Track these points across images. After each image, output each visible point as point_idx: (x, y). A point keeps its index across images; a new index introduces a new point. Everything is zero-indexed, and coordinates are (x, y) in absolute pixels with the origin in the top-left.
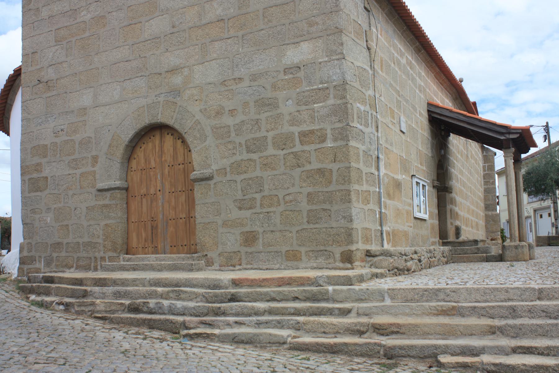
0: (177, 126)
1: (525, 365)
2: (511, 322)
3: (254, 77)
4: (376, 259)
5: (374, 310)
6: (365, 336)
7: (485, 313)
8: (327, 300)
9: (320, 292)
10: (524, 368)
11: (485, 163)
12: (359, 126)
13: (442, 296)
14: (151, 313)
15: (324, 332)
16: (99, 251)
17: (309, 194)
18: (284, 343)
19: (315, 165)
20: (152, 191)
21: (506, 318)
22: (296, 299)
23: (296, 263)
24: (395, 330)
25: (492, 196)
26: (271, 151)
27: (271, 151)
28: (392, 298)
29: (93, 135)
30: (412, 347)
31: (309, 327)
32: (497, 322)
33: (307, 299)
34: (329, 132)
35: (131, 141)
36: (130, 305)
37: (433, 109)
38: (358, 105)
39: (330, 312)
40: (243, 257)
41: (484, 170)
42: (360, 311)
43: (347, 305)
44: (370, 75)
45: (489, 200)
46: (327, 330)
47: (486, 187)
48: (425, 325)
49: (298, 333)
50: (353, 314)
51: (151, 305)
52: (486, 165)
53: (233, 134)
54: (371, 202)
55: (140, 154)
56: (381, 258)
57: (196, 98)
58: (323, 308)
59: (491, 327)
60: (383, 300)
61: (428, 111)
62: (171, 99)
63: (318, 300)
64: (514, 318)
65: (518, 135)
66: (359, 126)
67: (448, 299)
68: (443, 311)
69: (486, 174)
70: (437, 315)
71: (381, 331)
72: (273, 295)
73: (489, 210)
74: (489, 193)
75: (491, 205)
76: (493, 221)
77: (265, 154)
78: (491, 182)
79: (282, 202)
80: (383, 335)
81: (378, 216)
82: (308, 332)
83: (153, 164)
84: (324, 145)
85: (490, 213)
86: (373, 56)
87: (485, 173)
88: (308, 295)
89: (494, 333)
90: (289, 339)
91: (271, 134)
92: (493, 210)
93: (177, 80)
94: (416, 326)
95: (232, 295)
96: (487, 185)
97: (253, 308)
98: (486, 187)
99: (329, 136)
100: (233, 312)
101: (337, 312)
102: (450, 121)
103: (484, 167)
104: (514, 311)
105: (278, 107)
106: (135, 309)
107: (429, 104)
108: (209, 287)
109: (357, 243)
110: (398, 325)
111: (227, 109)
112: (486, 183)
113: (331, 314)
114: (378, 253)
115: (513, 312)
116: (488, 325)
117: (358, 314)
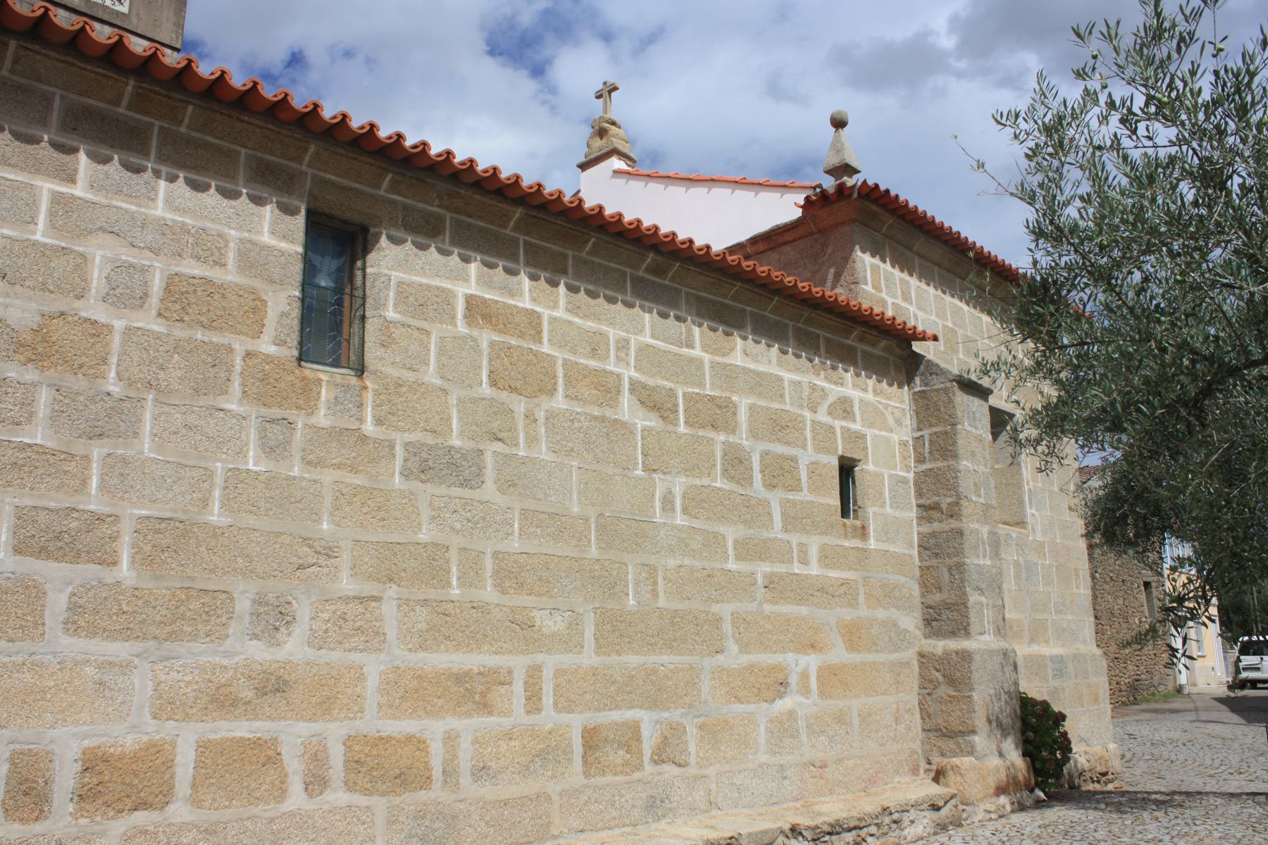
11: (920, 429)
25: (950, 569)
41: (920, 460)
45: (940, 589)
47: (926, 528)
52: (926, 433)
69: (926, 473)
74: (937, 555)
75: (949, 606)
76: (951, 682)
78: (944, 506)
85: (940, 646)
87: (924, 467)
92: (953, 634)
96: (930, 520)
112: (928, 510)
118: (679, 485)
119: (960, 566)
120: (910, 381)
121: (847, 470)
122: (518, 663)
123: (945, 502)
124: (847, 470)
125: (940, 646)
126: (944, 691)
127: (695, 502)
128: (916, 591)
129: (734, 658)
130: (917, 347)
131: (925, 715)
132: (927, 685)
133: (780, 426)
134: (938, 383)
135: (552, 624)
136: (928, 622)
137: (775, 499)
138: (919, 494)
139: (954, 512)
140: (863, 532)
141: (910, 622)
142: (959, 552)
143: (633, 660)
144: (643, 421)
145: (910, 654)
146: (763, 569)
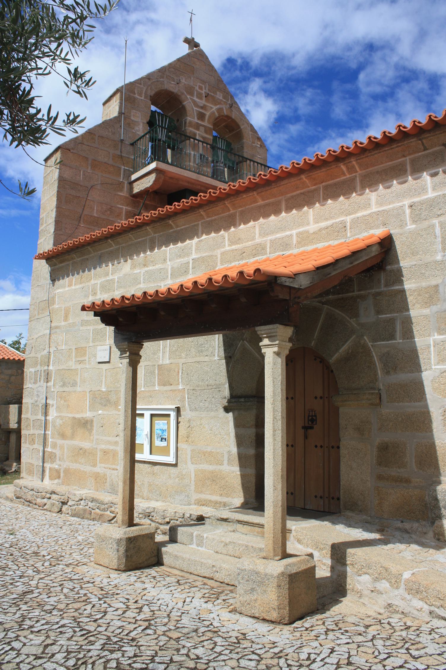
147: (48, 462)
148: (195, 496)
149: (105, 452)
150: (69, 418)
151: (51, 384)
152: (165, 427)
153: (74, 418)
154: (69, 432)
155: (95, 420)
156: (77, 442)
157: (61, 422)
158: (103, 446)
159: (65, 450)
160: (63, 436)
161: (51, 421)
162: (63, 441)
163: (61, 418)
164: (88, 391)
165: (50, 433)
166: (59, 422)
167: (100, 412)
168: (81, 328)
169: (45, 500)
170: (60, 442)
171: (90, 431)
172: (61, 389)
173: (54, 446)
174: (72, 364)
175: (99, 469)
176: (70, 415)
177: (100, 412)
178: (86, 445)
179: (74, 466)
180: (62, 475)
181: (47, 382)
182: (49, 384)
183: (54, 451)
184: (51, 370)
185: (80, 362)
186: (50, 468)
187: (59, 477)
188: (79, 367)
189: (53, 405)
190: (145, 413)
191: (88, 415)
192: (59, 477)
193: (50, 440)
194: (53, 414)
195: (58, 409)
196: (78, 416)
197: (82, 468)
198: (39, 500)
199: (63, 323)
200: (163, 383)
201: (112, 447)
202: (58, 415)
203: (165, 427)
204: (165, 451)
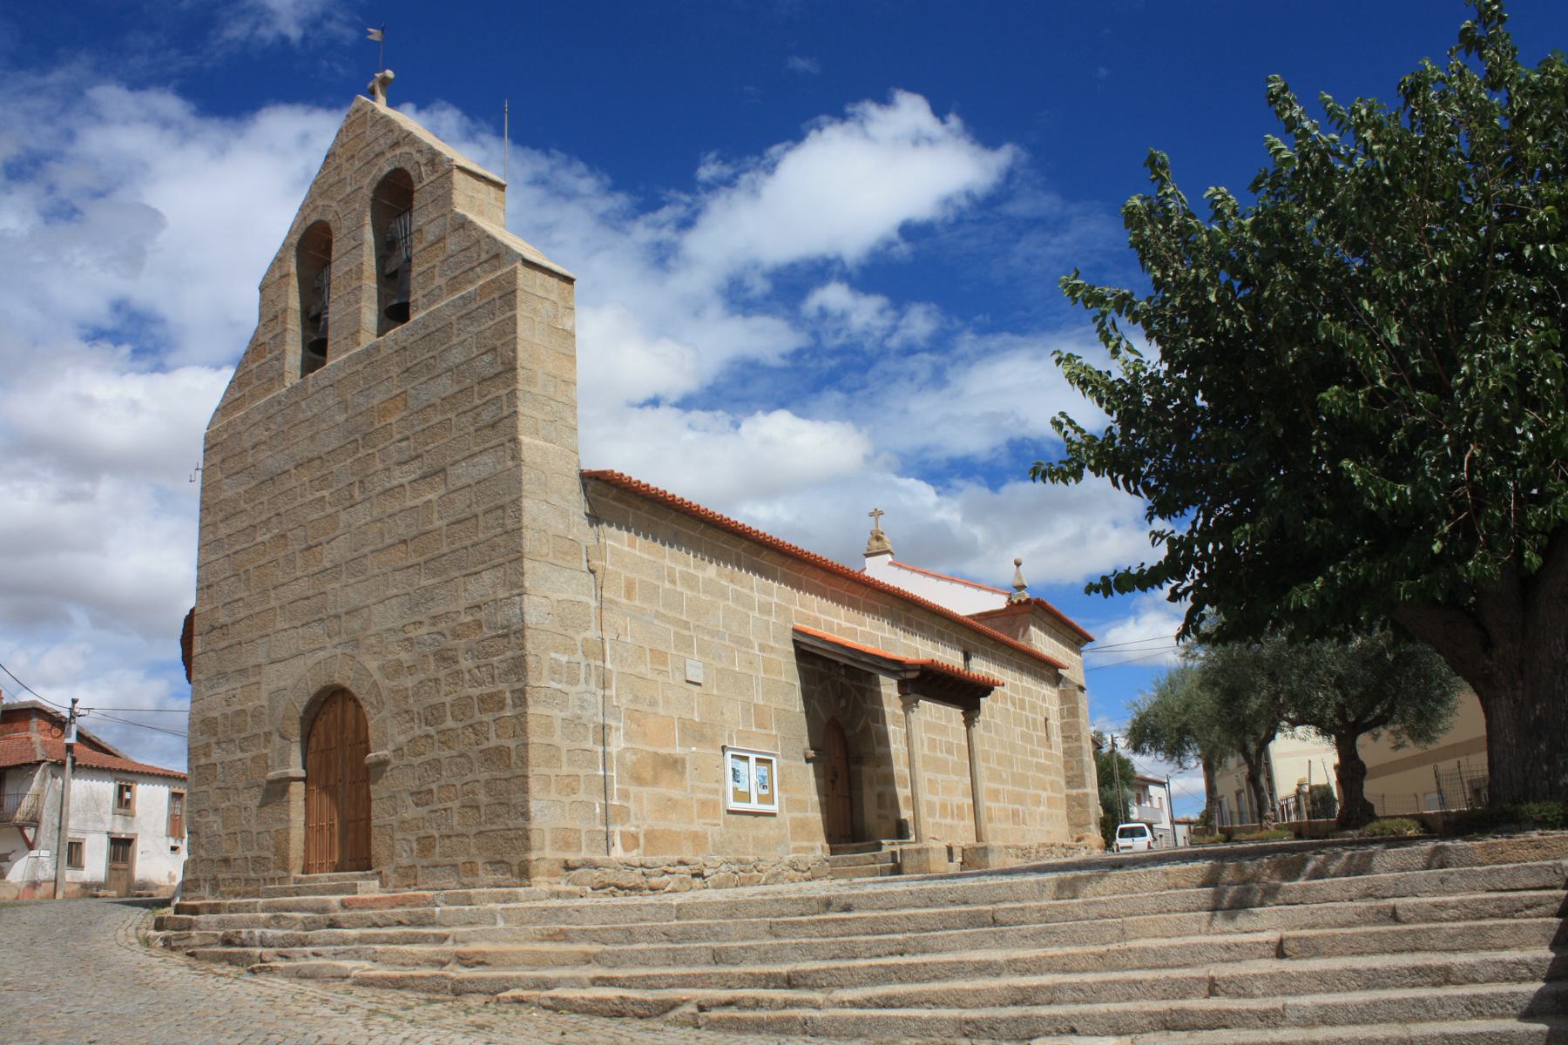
0: (353, 690)
1: (583, 998)
2: (625, 947)
3: (435, 619)
4: (574, 873)
5: (473, 936)
6: (447, 967)
7: (597, 938)
8: (433, 924)
9: (427, 915)
10: (581, 1002)
12: (554, 685)
13: (563, 917)
14: (243, 945)
15: (403, 964)
16: (268, 870)
17: (487, 782)
18: (347, 977)
19: (494, 742)
20: (332, 782)
21: (622, 943)
22: (400, 923)
23: (471, 879)
24: (481, 959)
26: (450, 723)
27: (450, 723)
28: (506, 920)
29: (266, 703)
30: (482, 980)
31: (386, 957)
32: (596, 948)
33: (411, 924)
34: (508, 695)
35: (307, 710)
36: (224, 936)
37: (800, 638)
38: (553, 655)
39: (424, 939)
40: (420, 873)
41: (1062, 718)
42: (457, 938)
43: (445, 931)
44: (592, 610)
46: (406, 961)
47: (1066, 746)
48: (513, 953)
49: (376, 965)
50: (450, 942)
51: (244, 936)
53: (411, 700)
54: (582, 790)
55: (320, 727)
56: (582, 870)
57: (375, 649)
58: (418, 934)
59: (587, 954)
60: (495, 924)
61: (795, 641)
62: (348, 651)
63: (423, 925)
64: (630, 943)
65: (917, 674)
66: (554, 685)
67: (570, 920)
68: (549, 935)
70: (542, 941)
71: (465, 962)
72: (376, 919)
73: (1073, 787)
76: (1080, 805)
77: (443, 727)
79: (460, 794)
80: (467, 966)
81: (598, 810)
82: (386, 963)
83: (333, 744)
84: (503, 713)
85: (1074, 792)
86: (599, 580)
88: (413, 918)
89: (589, 962)
90: (355, 972)
91: (448, 700)
92: (1079, 787)
93: (356, 624)
94: (504, 954)
95: (331, 920)
97: (342, 936)
98: (1066, 746)
99: (509, 701)
100: (321, 940)
101: (432, 939)
102: (826, 655)
103: (1062, 710)
104: (631, 933)
105: (457, 662)
106: (228, 942)
107: (795, 631)
108: (317, 911)
109: (541, 849)
110: (484, 954)
111: (405, 665)
113: (426, 942)
114: (577, 864)
115: (630, 935)
116: (582, 952)
117: (455, 942)
118: (1018, 730)
119: (1081, 761)
120: (1057, 685)
121: (1046, 720)
122: (1001, 787)
123: (1074, 735)
124: (1046, 720)
125: (1074, 792)
126: (1077, 809)
127: (1025, 737)
128: (1062, 770)
129: (1032, 791)
130: (1060, 671)
131: (1069, 819)
132: (1070, 807)
133: (1033, 707)
134: (1070, 687)
135: (1005, 776)
136: (1068, 783)
137: (1034, 734)
138: (1063, 731)
139: (1078, 739)
140: (1051, 748)
141: (1063, 783)
142: (1081, 755)
143: (1017, 789)
144: (1012, 709)
145: (1063, 796)
146: (1035, 760)
147: (615, 823)
148: (792, 845)
149: (703, 803)
150: (648, 752)
151: (612, 692)
152: (766, 774)
153: (656, 754)
154: (648, 774)
155: (687, 758)
156: (662, 790)
157: (634, 757)
158: (701, 796)
159: (645, 802)
160: (639, 780)
161: (614, 755)
162: (641, 789)
163: (635, 751)
164: (676, 717)
165: (614, 774)
166: (630, 758)
167: (694, 749)
168: (656, 622)
169: (666, 877)
170: (633, 789)
171: (682, 773)
172: (632, 707)
173: (625, 795)
174: (645, 669)
175: (697, 826)
176: (651, 749)
177: (694, 749)
178: (676, 794)
179: (661, 825)
180: (642, 841)
181: (604, 688)
182: (607, 692)
183: (625, 804)
184: (610, 671)
185: (660, 672)
186: (622, 834)
187: (637, 845)
188: (660, 678)
189: (618, 729)
190: (753, 758)
191: (678, 751)
192: (637, 845)
193: (616, 786)
194: (617, 744)
195: (628, 736)
196: (663, 751)
197: (675, 827)
198: (654, 881)
199: (624, 601)
200: (760, 726)
201: (711, 797)
202: (629, 745)
203: (766, 774)
204: (768, 799)
